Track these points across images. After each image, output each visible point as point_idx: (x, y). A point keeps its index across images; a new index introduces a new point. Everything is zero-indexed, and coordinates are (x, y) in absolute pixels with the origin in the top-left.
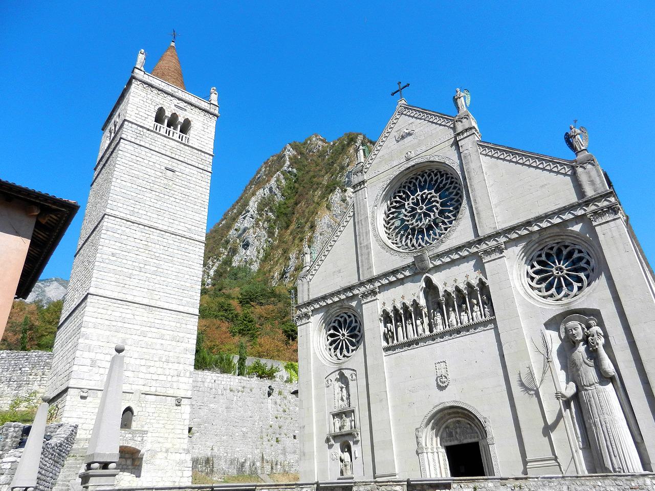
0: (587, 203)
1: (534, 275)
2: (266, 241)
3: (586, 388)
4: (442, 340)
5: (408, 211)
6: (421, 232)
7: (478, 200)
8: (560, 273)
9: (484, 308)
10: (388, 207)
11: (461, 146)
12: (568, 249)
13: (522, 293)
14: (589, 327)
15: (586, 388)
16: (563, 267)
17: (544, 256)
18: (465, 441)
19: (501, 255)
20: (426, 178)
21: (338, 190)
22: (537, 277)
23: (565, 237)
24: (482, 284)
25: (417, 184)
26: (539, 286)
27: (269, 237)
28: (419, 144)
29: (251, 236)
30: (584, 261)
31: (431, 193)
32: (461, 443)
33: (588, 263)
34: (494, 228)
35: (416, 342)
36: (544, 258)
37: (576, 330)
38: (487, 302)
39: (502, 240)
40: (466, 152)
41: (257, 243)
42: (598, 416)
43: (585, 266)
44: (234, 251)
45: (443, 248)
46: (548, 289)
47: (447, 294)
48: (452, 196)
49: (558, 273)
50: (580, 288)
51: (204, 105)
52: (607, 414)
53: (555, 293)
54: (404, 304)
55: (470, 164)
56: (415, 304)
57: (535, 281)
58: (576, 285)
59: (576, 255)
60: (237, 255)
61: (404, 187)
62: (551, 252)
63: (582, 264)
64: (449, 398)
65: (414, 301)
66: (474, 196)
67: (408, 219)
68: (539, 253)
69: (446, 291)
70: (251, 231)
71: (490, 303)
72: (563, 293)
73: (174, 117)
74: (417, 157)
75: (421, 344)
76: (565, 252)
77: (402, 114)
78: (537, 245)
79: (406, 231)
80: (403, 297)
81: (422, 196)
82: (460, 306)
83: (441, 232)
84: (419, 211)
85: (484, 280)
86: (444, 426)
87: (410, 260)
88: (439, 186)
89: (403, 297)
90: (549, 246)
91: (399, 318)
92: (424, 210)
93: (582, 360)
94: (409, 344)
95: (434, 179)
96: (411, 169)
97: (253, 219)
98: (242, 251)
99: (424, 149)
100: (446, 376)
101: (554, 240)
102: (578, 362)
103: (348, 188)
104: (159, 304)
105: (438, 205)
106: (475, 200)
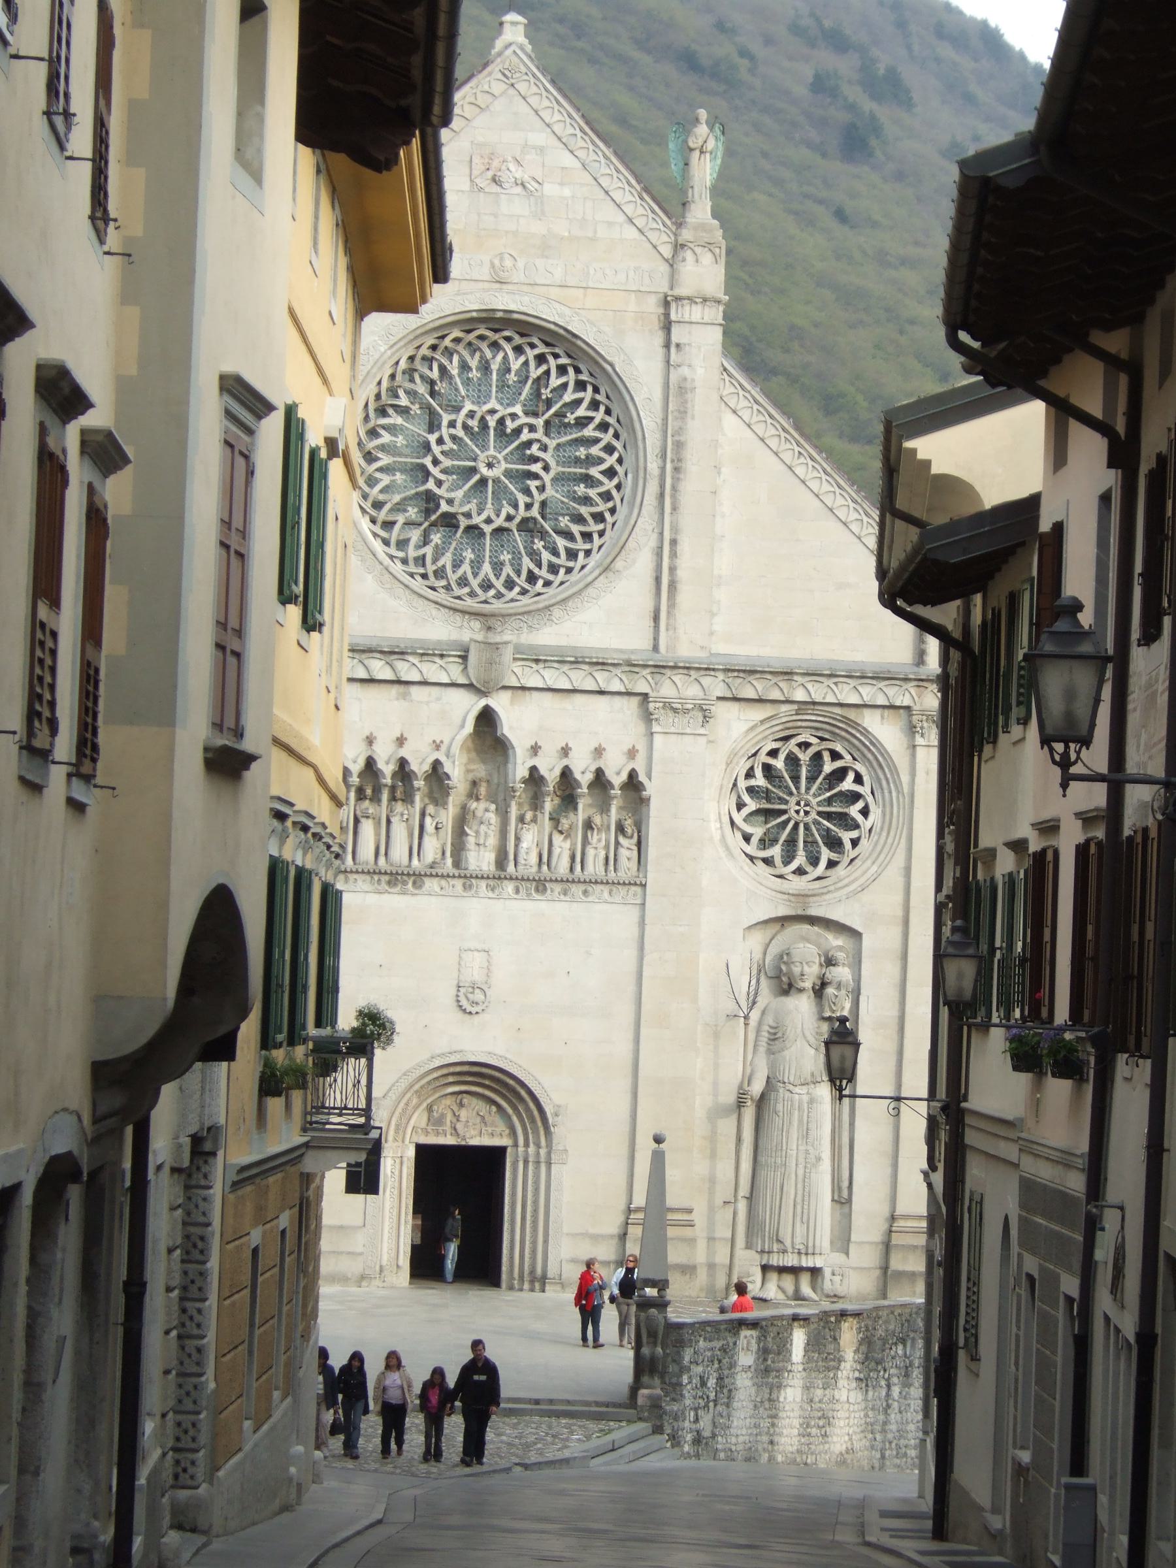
0: (921, 683)
1: (746, 798)
3: (791, 1087)
4: (490, 894)
5: (445, 448)
6: (473, 531)
7: (684, 546)
8: (802, 813)
9: (617, 843)
10: (378, 396)
11: (678, 345)
12: (839, 764)
13: (717, 836)
14: (830, 962)
15: (791, 1087)
16: (814, 801)
17: (782, 756)
18: (475, 1142)
19: (702, 731)
20: (601, 461)
22: (752, 805)
23: (843, 734)
24: (633, 784)
25: (495, 367)
26: (748, 829)
28: (546, 247)
30: (860, 805)
31: (532, 428)
32: (463, 1143)
33: (865, 812)
34: (702, 648)
35: (418, 878)
36: (779, 763)
37: (810, 967)
38: (629, 830)
39: (716, 686)
40: (685, 371)
42: (795, 1147)
43: (859, 818)
45: (547, 636)
46: (764, 843)
47: (535, 778)
48: (594, 472)
49: (797, 812)
50: (832, 864)
52: (813, 1146)
53: (778, 860)
54: (403, 763)
55: (689, 421)
56: (436, 773)
57: (745, 811)
58: (826, 854)
59: (848, 784)
61: (449, 353)
62: (801, 756)
63: (854, 811)
65: (436, 764)
66: (675, 529)
67: (442, 477)
68: (775, 745)
69: (533, 770)
71: (636, 835)
72: (794, 865)
74: (525, 288)
75: (431, 884)
76: (829, 767)
77: (512, 85)
78: (780, 727)
79: (428, 512)
80: (401, 741)
81: (501, 422)
82: (556, 821)
83: (536, 570)
84: (484, 471)
85: (642, 778)
86: (429, 1101)
88: (560, 415)
89: (401, 741)
90: (800, 739)
91: (369, 792)
92: (497, 472)
93: (799, 1030)
94: (396, 878)
95: (555, 382)
96: (499, 315)
99: (558, 275)
100: (486, 989)
101: (817, 729)
102: (790, 1033)
105: (548, 478)
106: (674, 542)
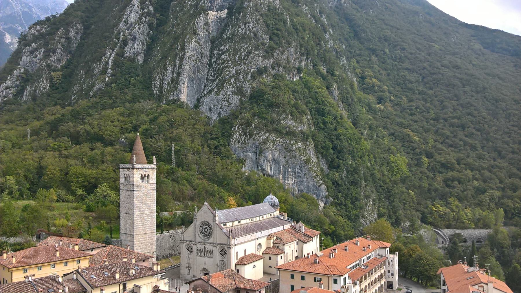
2: (149, 33)
21: (202, 15)
27: (150, 29)
29: (137, 31)
41: (142, 37)
44: (125, 43)
51: (152, 166)
60: (127, 47)
64: (205, 267)
70: (137, 26)
73: (145, 175)
87: (202, 241)
97: (137, 13)
98: (130, 43)
103: (209, 12)
104: (148, 232)
